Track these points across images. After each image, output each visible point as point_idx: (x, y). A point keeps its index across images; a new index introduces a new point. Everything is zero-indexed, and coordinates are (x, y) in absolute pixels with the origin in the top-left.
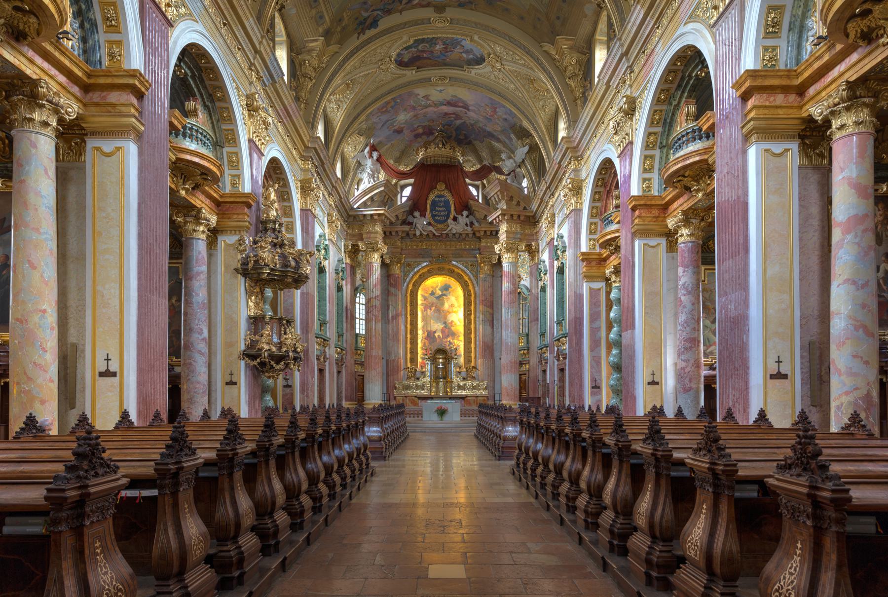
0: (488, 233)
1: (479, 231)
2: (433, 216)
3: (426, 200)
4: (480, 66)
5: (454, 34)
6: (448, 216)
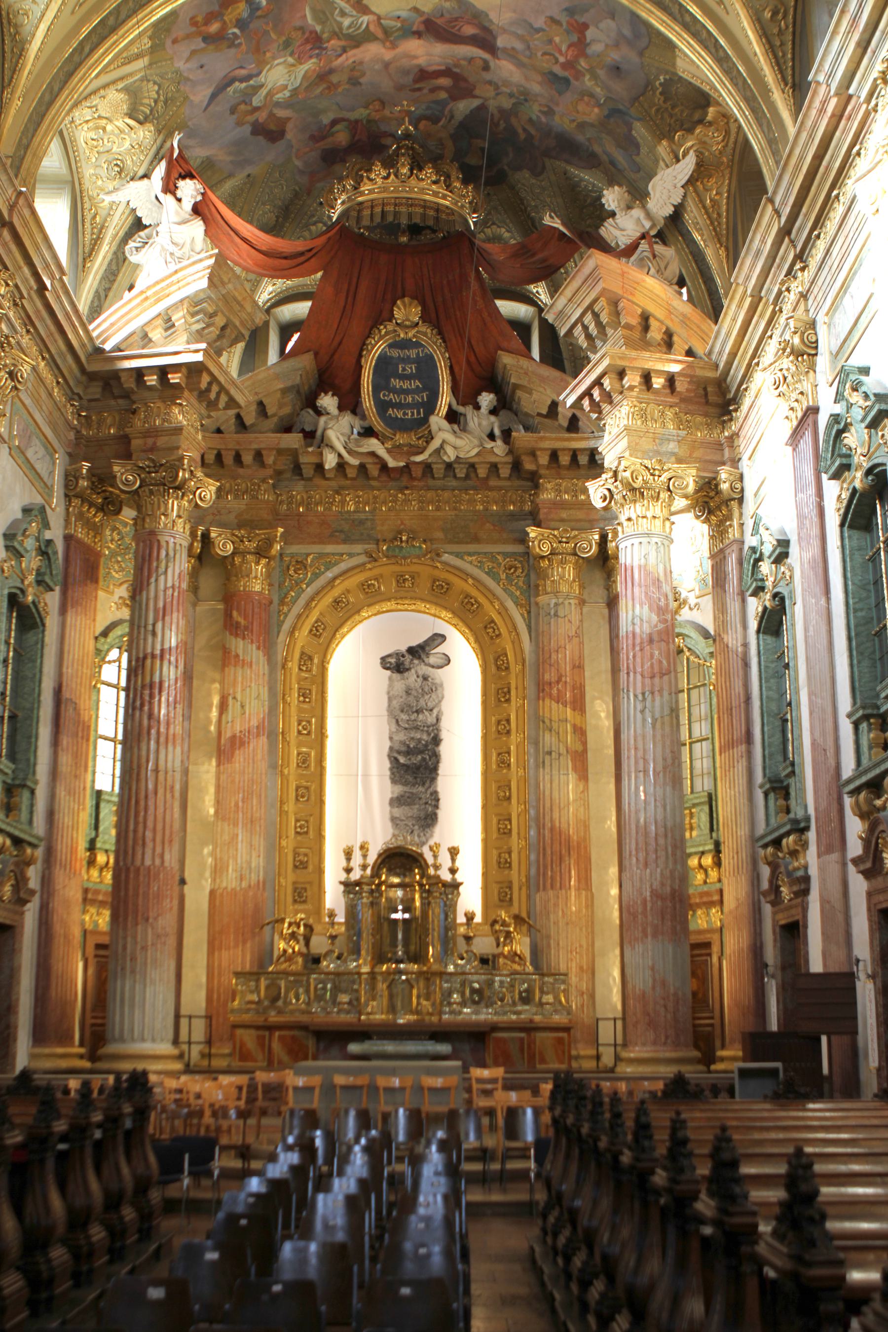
1: (533, 454)
2: (382, 407)
3: (360, 356)
6: (430, 407)
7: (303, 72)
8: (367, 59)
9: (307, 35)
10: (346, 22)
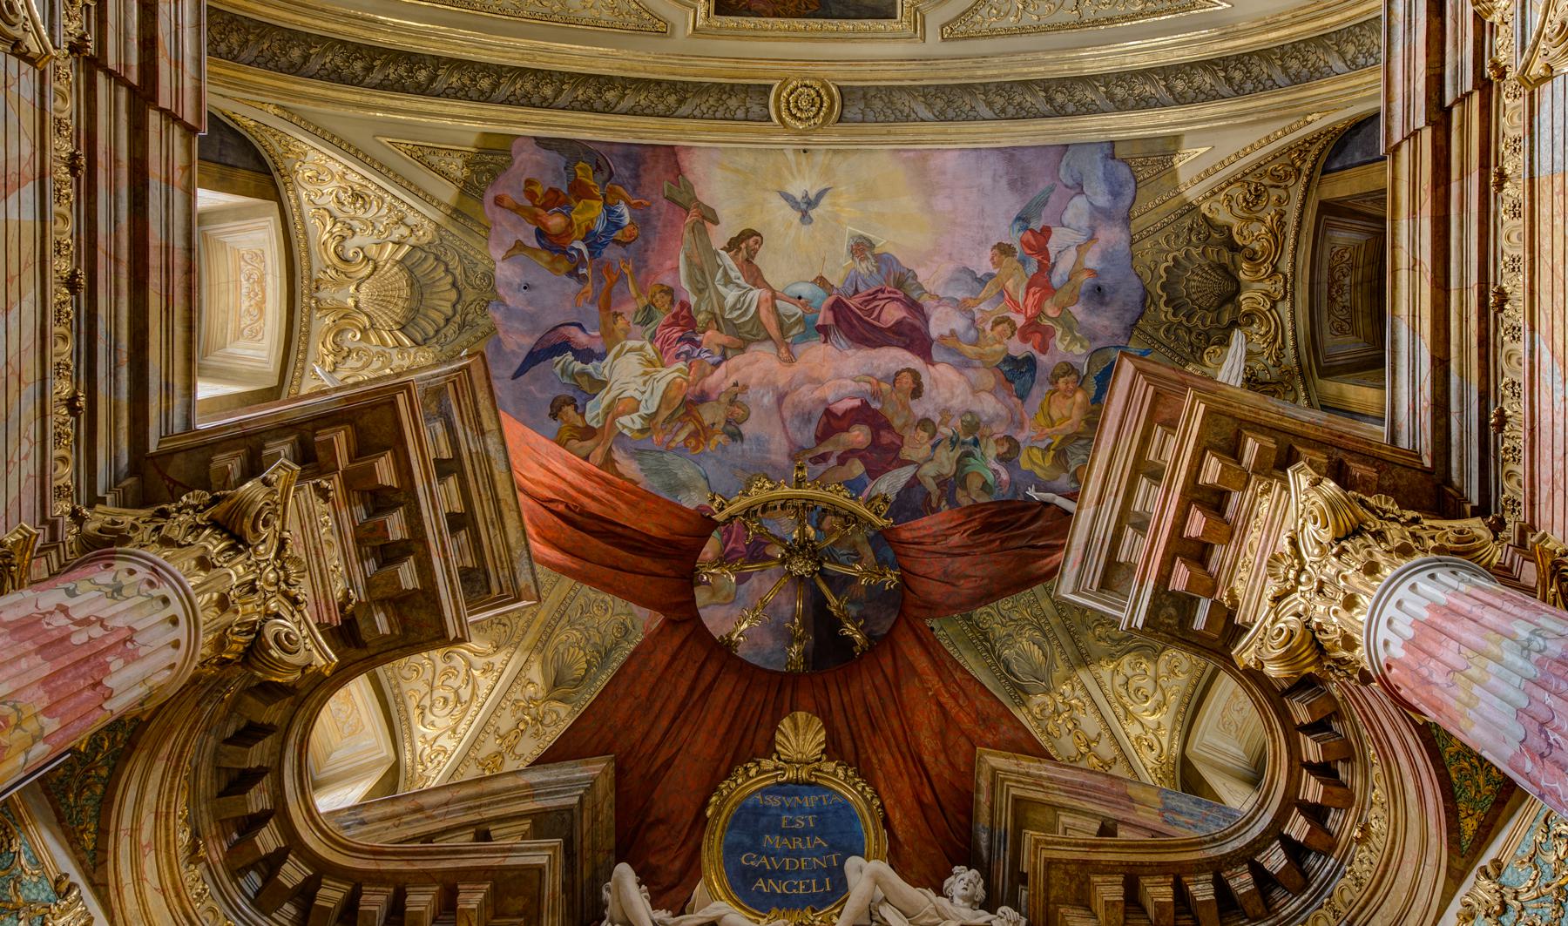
7: (662, 385)
8: (753, 381)
9: (676, 308)
10: (731, 296)
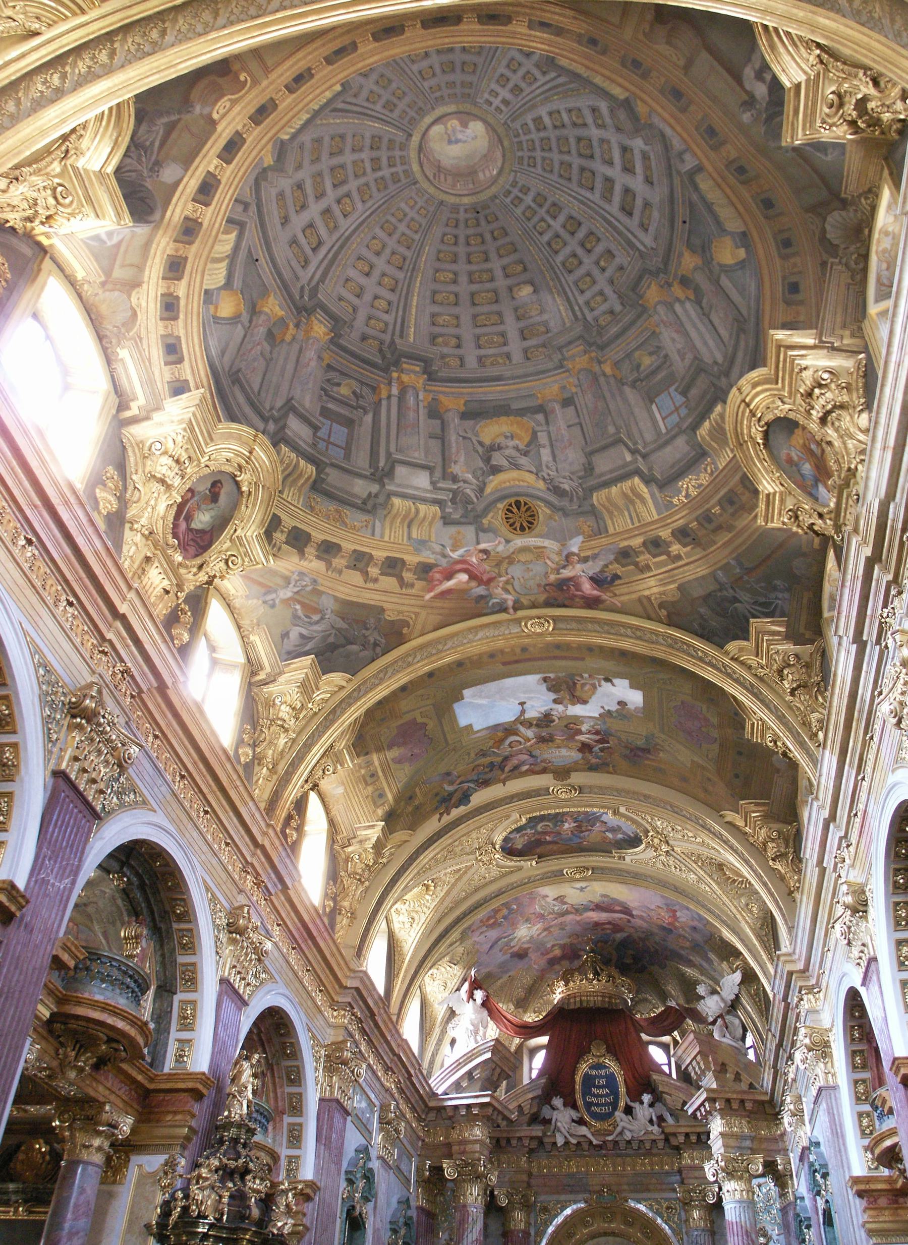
0: (694, 1138)
4: (636, 850)
5: (589, 806)
